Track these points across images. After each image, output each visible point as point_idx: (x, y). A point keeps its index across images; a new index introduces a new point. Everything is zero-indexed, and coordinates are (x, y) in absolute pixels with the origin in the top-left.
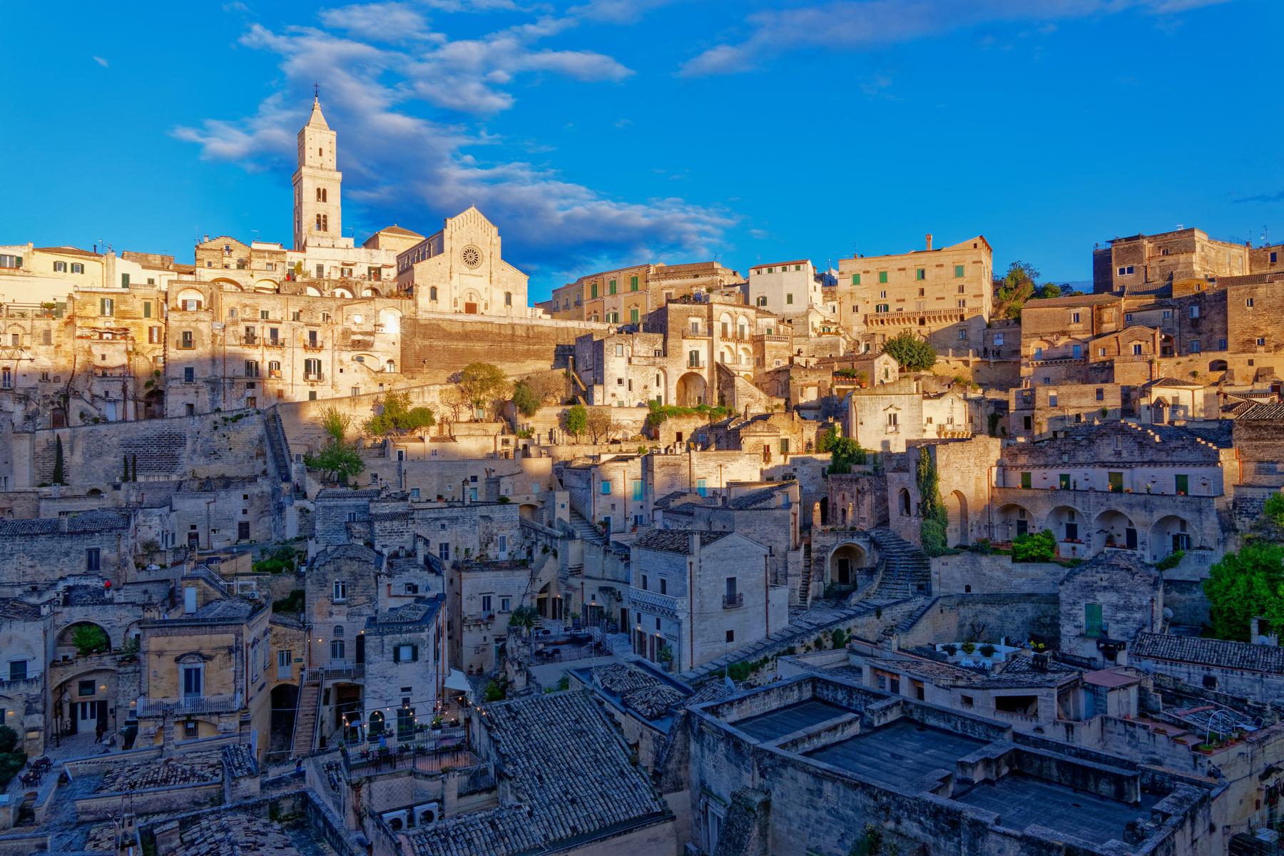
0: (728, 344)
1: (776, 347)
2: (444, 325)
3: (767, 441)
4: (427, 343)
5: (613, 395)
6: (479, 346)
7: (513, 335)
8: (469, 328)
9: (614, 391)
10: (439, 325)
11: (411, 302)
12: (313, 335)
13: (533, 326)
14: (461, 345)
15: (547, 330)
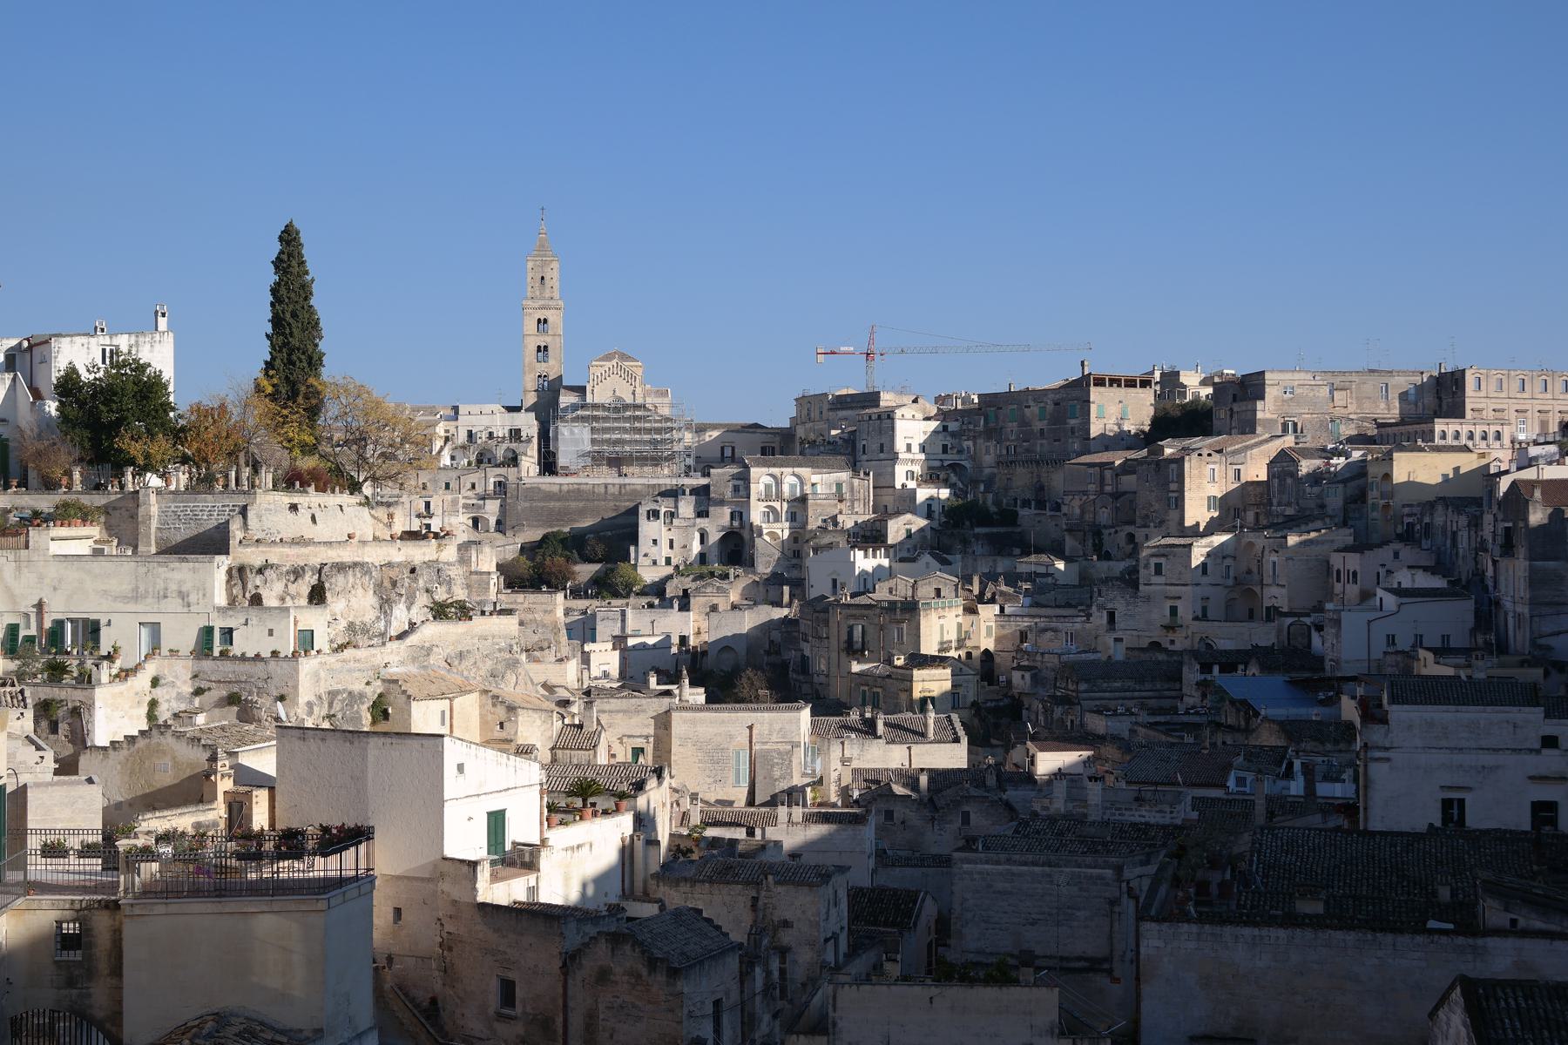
0: (770, 503)
1: (820, 505)
2: (543, 487)
3: (715, 601)
4: (527, 505)
5: (646, 555)
6: (573, 505)
7: (606, 492)
8: (565, 488)
9: (648, 551)
10: (539, 489)
11: (516, 469)
12: (428, 505)
13: (625, 485)
14: (558, 504)
15: (639, 487)
